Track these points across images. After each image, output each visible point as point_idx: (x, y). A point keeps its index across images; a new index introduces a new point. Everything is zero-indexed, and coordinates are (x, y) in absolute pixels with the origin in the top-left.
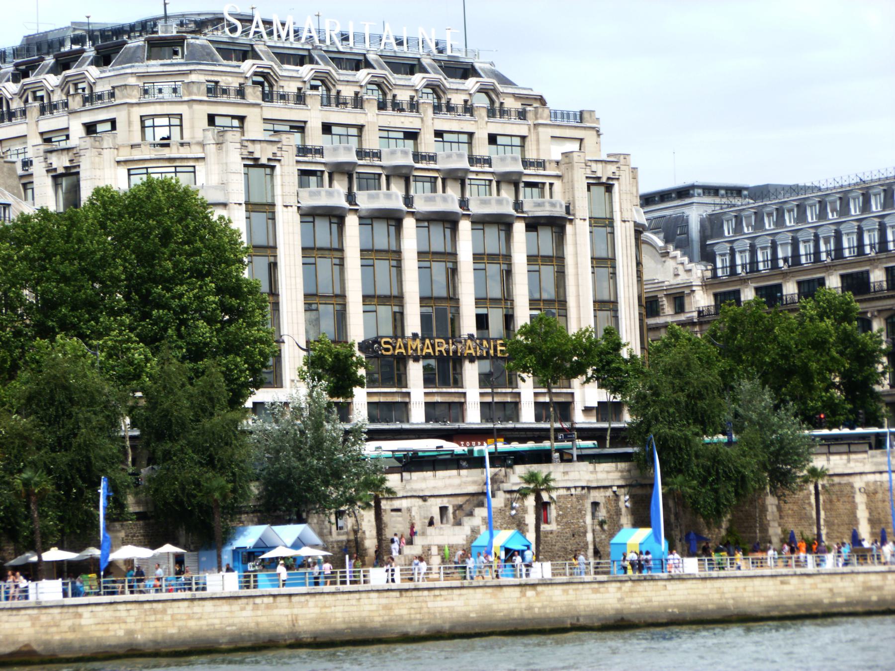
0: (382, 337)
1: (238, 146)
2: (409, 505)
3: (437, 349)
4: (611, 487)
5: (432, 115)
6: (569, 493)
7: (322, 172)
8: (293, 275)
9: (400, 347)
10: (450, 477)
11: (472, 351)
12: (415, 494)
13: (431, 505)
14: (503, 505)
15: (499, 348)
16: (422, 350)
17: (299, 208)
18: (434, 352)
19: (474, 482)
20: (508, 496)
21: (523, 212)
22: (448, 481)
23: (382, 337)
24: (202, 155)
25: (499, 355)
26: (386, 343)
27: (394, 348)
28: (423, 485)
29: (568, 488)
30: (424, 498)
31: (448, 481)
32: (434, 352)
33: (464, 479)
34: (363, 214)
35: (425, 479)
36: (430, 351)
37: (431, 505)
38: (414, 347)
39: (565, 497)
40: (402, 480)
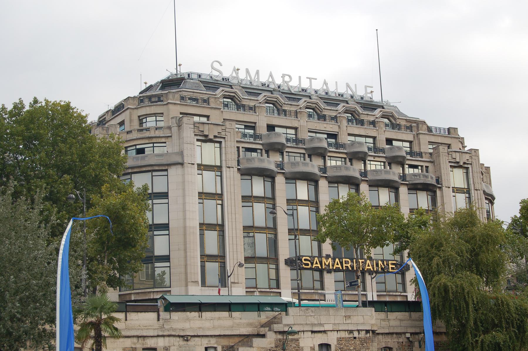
0: (303, 256)
1: (192, 126)
2: (167, 345)
3: (344, 265)
4: (405, 333)
5: (346, 125)
6: (351, 335)
7: (261, 150)
8: (233, 212)
9: (316, 263)
10: (219, 318)
11: (371, 267)
12: (173, 333)
13: (195, 346)
14: (273, 345)
15: (390, 266)
16: (333, 266)
17: (238, 169)
18: (342, 267)
19: (250, 325)
20: (280, 337)
21: (406, 181)
22: (217, 323)
23: (303, 256)
24: (170, 135)
25: (390, 270)
26: (305, 260)
27: (312, 264)
28: (187, 325)
29: (351, 332)
30: (186, 338)
31: (217, 323)
32: (342, 267)
33: (238, 321)
34: (288, 176)
35: (188, 319)
36: (340, 266)
37: (195, 346)
38: (327, 264)
39: (347, 340)
40: (158, 320)
